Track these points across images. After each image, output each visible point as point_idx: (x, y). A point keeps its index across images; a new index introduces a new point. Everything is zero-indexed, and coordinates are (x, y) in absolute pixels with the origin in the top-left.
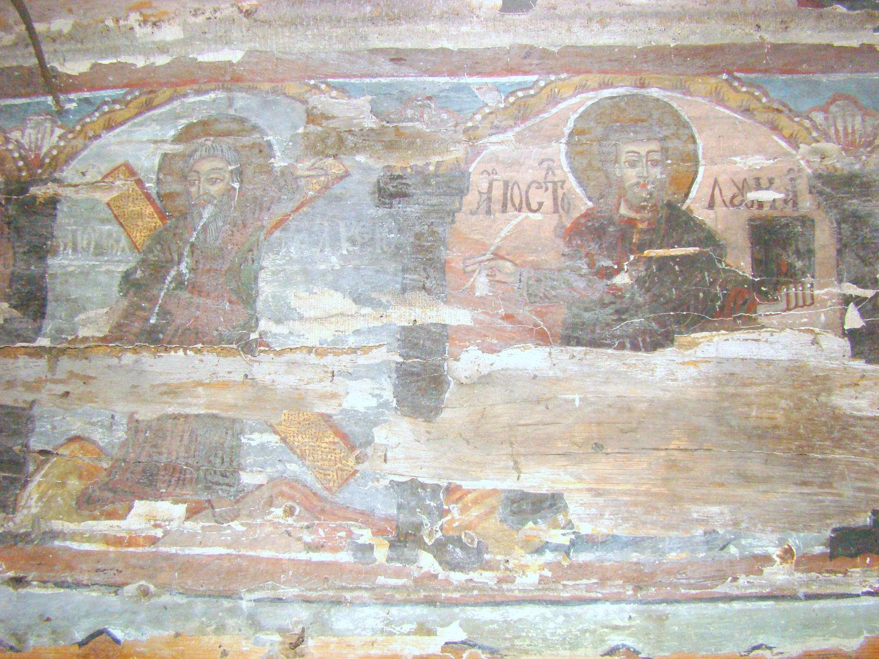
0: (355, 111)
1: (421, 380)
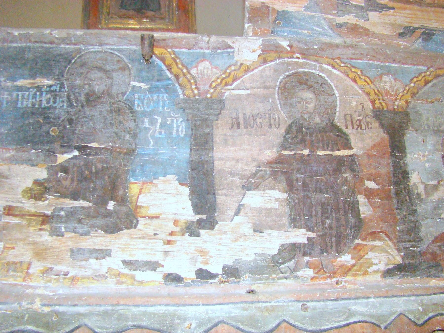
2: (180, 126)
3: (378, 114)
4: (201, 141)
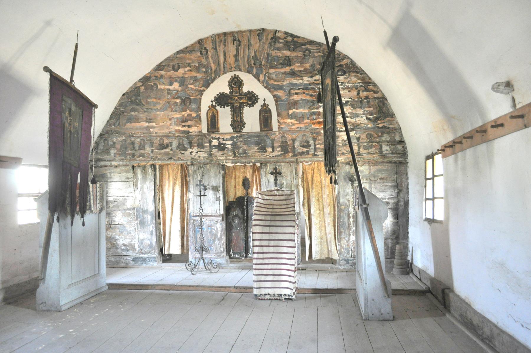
1: (152, 152)
2: (270, 142)
4: (273, 144)
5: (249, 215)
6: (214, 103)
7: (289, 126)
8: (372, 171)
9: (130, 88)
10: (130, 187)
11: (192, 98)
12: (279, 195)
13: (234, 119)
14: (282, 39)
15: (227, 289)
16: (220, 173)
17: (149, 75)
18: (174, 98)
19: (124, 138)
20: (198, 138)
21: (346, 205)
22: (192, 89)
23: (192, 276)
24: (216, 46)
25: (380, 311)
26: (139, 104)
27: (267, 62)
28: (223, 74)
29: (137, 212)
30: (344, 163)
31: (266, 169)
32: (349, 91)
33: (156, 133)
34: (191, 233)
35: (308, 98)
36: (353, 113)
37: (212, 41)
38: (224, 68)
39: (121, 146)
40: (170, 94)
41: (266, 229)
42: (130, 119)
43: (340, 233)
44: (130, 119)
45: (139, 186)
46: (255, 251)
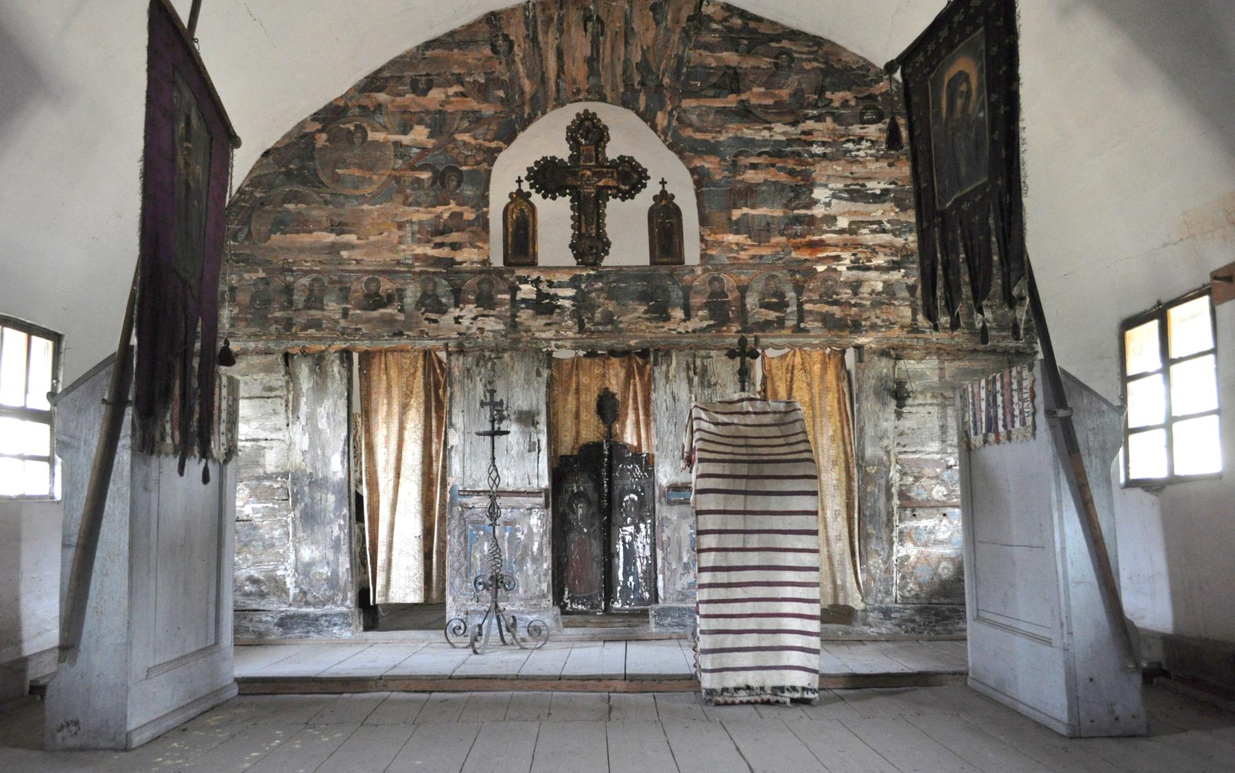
0: (336, 278)
1: (345, 314)
2: (681, 294)
3: (738, 287)
4: (686, 298)
5: (616, 492)
6: (526, 187)
7: (731, 250)
8: (947, 374)
9: (284, 137)
10: (275, 412)
11: (464, 168)
12: (755, 413)
13: (579, 229)
14: (715, 22)
15: (603, 683)
16: (539, 374)
17: (342, 104)
18: (413, 168)
19: (261, 274)
20: (478, 278)
21: (881, 462)
22: (465, 143)
23: (475, 657)
24: (535, 33)
25: (1112, 712)
26: (312, 181)
27: (678, 80)
28: (555, 107)
29: (294, 484)
30: (874, 352)
31: (668, 366)
32: (890, 165)
33: (358, 262)
34: (453, 542)
35: (783, 177)
36: (899, 222)
37: (527, 18)
38: (558, 91)
39: (253, 299)
40: (402, 156)
41: (737, 503)
42: (282, 222)
43: (865, 537)
44: (282, 222)
45: (304, 409)
46: (704, 564)
